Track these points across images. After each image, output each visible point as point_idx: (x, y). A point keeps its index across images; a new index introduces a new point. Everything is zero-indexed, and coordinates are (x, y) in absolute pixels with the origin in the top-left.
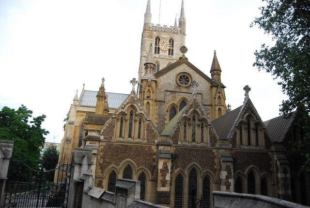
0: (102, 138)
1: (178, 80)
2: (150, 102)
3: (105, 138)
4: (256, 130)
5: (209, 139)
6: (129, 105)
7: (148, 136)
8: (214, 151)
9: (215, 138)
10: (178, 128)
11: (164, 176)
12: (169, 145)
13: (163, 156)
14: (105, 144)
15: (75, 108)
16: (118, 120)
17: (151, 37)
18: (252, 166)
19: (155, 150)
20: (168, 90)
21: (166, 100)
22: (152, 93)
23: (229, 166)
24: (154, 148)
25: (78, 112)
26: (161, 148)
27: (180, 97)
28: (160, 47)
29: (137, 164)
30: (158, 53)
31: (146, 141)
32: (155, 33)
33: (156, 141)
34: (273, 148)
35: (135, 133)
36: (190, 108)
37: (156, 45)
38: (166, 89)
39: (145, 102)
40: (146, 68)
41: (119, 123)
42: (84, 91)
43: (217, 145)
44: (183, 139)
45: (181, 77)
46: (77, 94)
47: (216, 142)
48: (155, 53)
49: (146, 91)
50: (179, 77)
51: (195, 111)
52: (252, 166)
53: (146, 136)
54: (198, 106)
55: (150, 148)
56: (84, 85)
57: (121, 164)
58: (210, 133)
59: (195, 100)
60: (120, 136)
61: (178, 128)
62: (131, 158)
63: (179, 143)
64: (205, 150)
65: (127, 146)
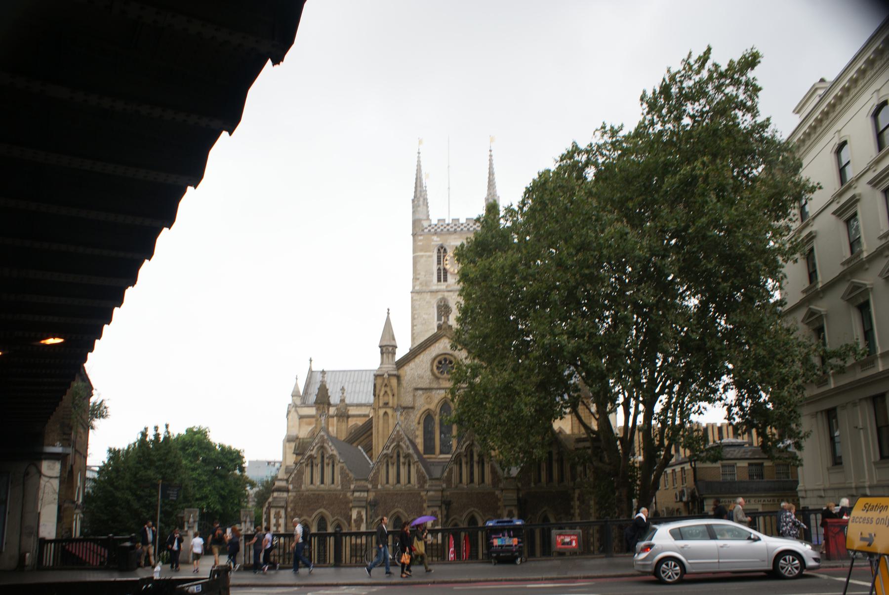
0: (291, 487)
1: (435, 368)
2: (390, 411)
3: (294, 487)
4: (481, 462)
5: (416, 479)
6: (319, 445)
7: (342, 481)
8: (423, 493)
9: (424, 477)
10: (378, 469)
11: (359, 526)
12: (368, 491)
13: (356, 504)
14: (294, 494)
15: (296, 411)
16: (307, 465)
17: (425, 249)
18: (472, 509)
19: (351, 498)
20: (419, 386)
21: (417, 405)
22: (391, 397)
23: (436, 512)
24: (349, 494)
25: (301, 417)
26: (357, 494)
27: (439, 397)
28: (448, 267)
29: (332, 514)
30: (445, 280)
31: (340, 487)
32: (435, 238)
33: (352, 487)
34: (501, 485)
35: (328, 479)
36: (392, 442)
37: (439, 263)
38: (414, 385)
39: (381, 412)
40: (382, 353)
41: (308, 469)
42: (311, 372)
43: (427, 486)
44: (384, 481)
45: (440, 362)
46: (296, 385)
47: (425, 482)
48: (439, 280)
49: (382, 393)
50: (436, 362)
51: (398, 446)
52: (472, 509)
53: (339, 482)
54: (402, 439)
55: (345, 495)
56: (311, 360)
57: (314, 516)
58: (418, 471)
59: (398, 432)
60: (312, 483)
61: (378, 469)
62: (324, 508)
63: (379, 487)
64: (411, 494)
65: (319, 495)
